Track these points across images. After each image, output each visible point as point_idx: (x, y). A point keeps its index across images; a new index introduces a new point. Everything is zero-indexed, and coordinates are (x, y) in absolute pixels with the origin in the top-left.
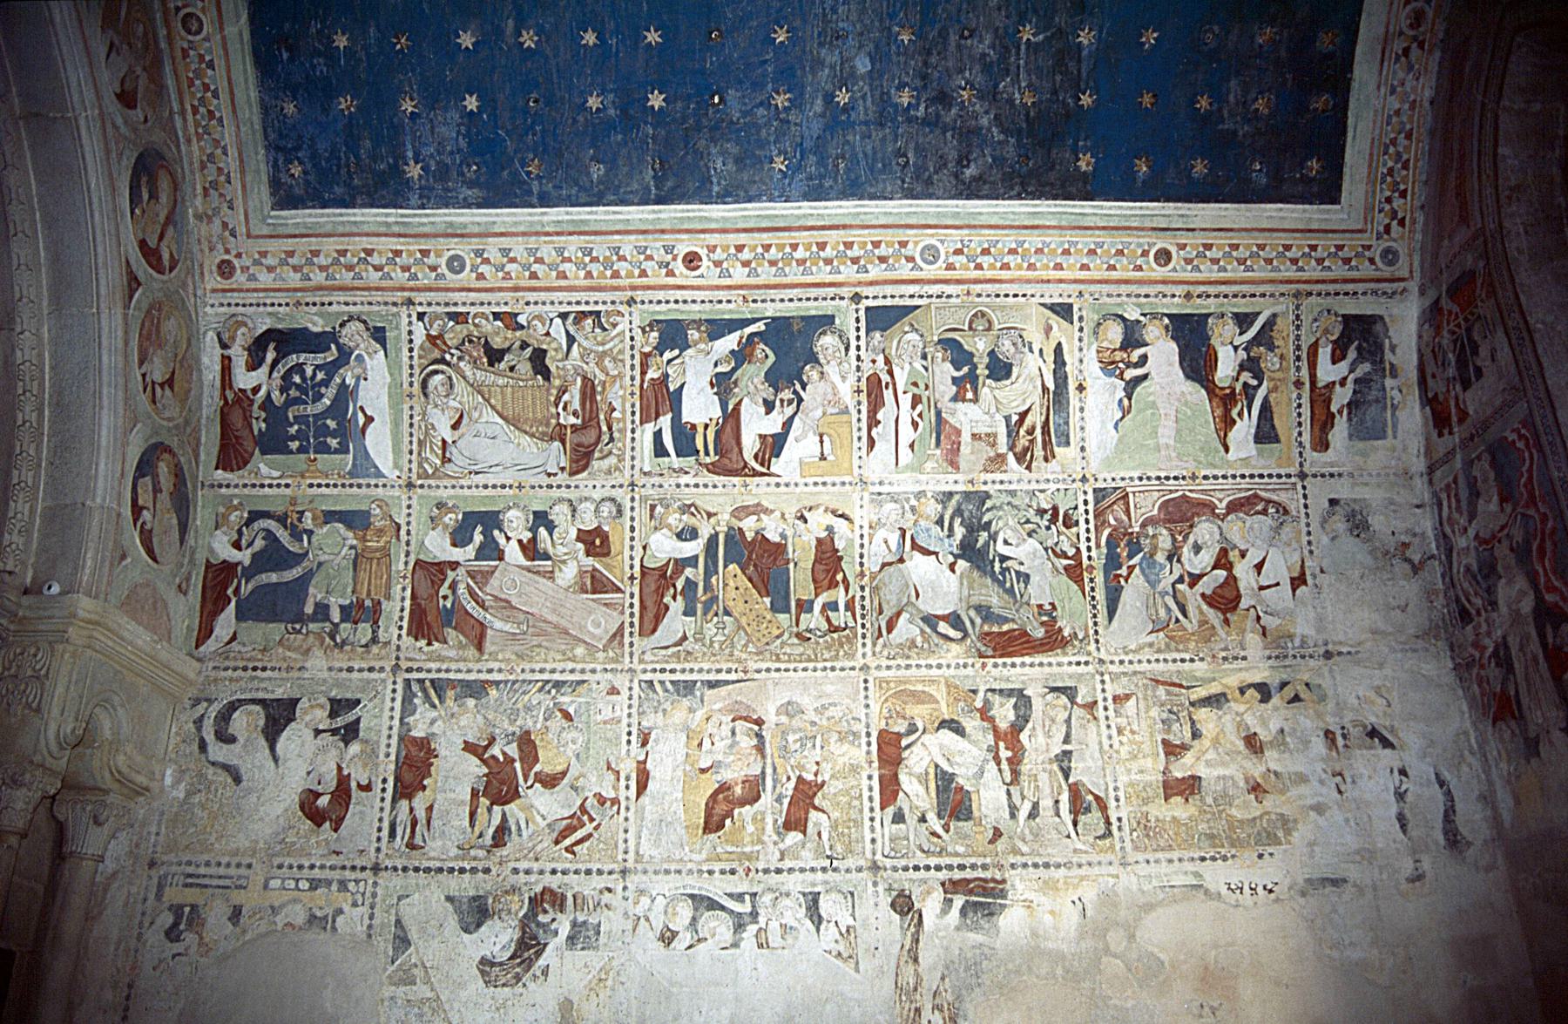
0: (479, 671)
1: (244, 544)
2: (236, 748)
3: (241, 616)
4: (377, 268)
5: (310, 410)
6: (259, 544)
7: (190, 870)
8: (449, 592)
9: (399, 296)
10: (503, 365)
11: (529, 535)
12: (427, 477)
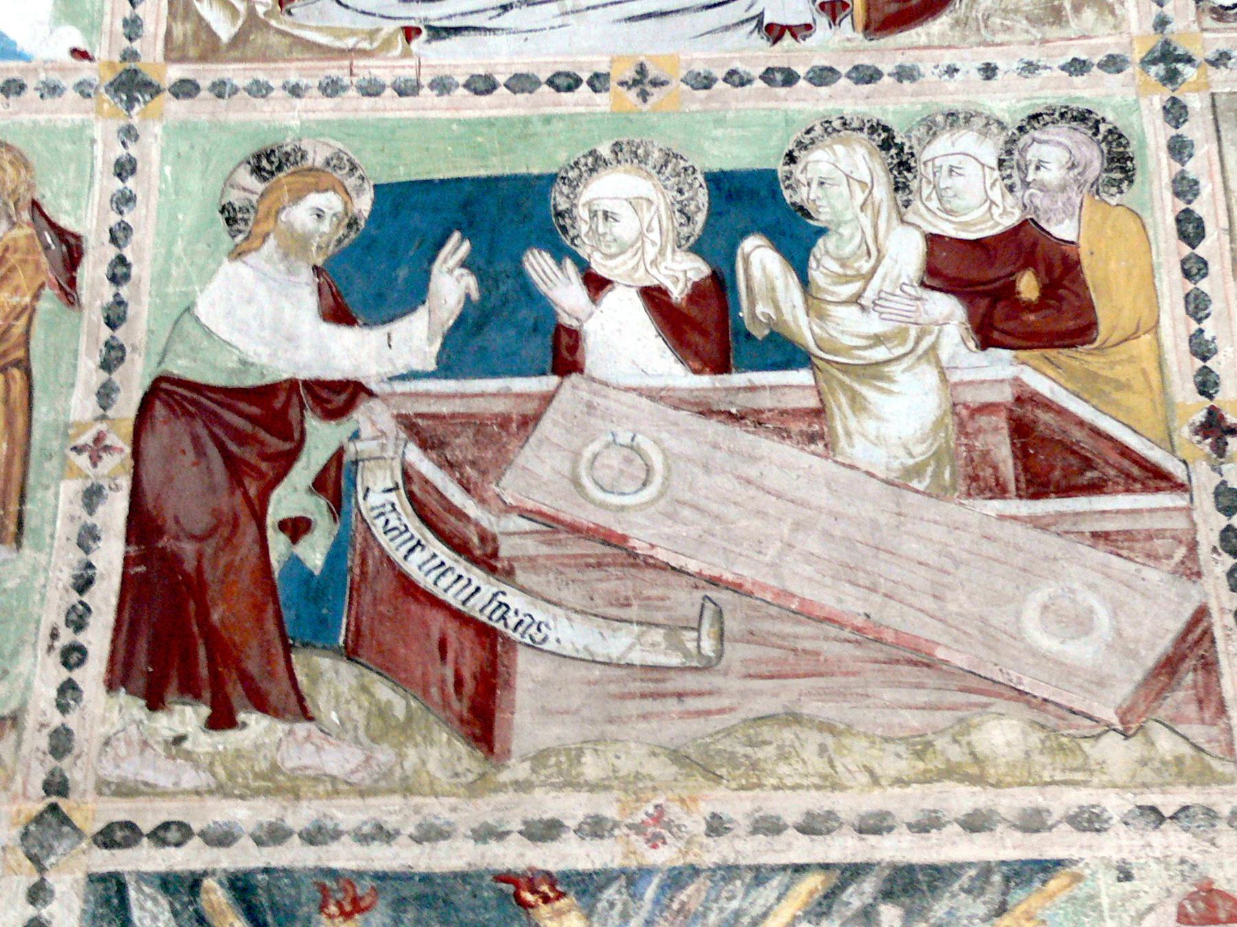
0: (486, 834)
8: (315, 508)
11: (696, 269)
12: (210, 49)
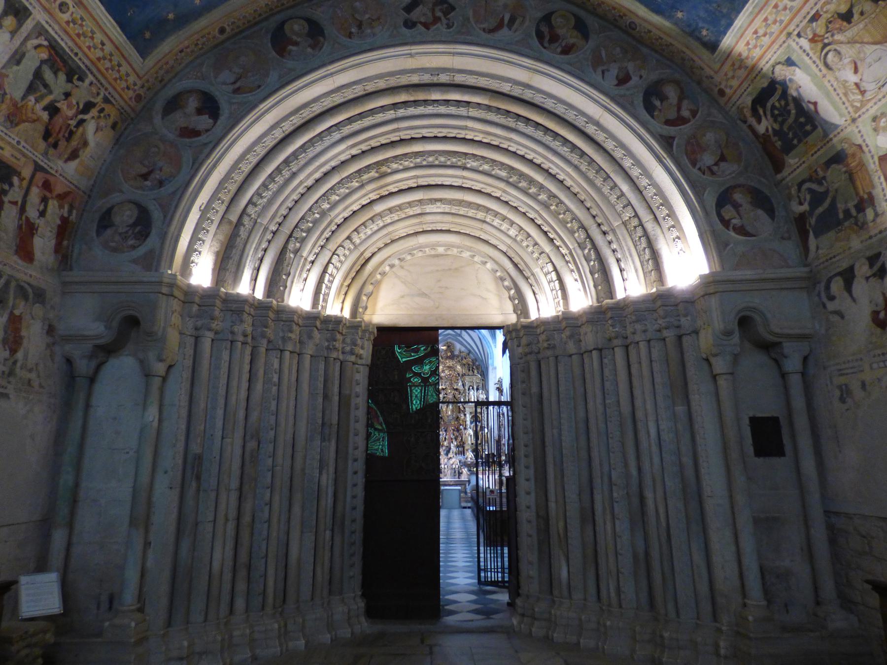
1: (802, 200)
2: (837, 301)
3: (817, 236)
4: (765, 35)
5: (791, 120)
6: (808, 197)
7: (839, 367)
9: (783, 37)
10: (856, 16)
